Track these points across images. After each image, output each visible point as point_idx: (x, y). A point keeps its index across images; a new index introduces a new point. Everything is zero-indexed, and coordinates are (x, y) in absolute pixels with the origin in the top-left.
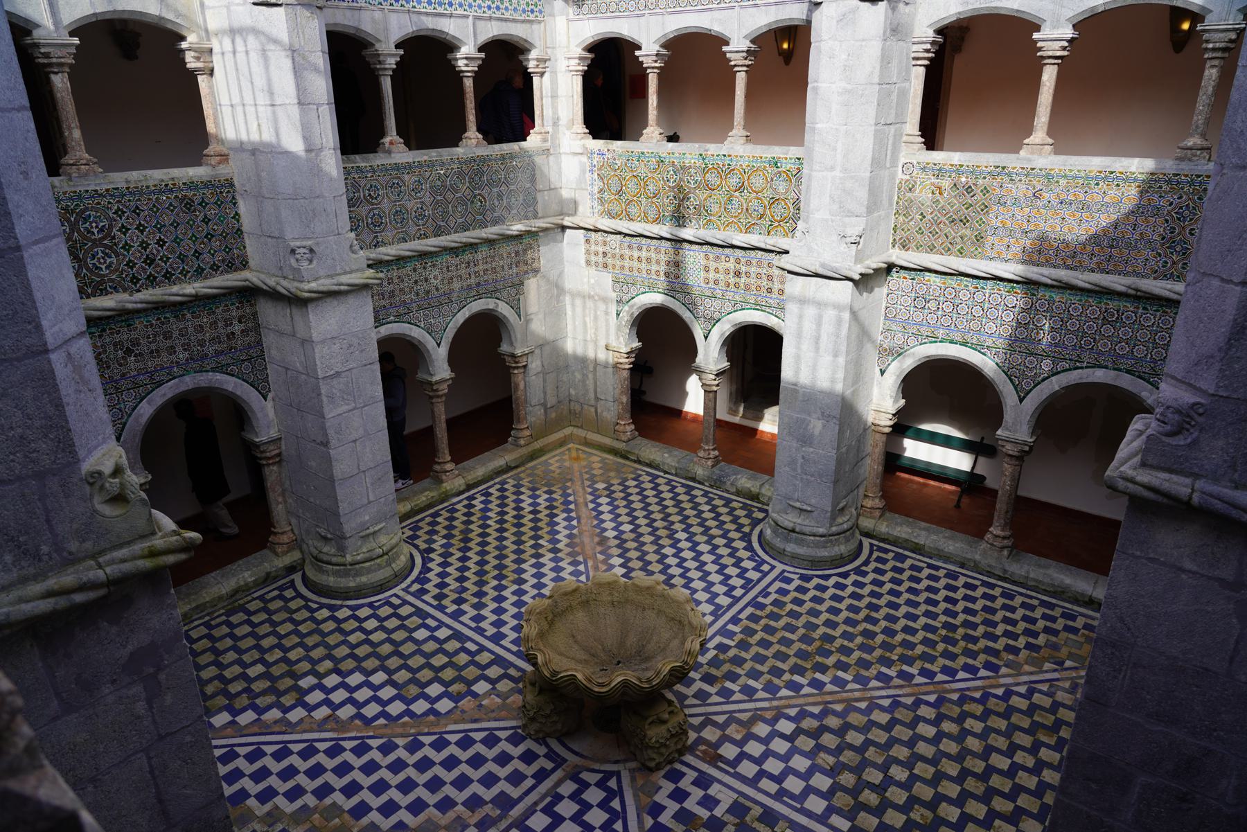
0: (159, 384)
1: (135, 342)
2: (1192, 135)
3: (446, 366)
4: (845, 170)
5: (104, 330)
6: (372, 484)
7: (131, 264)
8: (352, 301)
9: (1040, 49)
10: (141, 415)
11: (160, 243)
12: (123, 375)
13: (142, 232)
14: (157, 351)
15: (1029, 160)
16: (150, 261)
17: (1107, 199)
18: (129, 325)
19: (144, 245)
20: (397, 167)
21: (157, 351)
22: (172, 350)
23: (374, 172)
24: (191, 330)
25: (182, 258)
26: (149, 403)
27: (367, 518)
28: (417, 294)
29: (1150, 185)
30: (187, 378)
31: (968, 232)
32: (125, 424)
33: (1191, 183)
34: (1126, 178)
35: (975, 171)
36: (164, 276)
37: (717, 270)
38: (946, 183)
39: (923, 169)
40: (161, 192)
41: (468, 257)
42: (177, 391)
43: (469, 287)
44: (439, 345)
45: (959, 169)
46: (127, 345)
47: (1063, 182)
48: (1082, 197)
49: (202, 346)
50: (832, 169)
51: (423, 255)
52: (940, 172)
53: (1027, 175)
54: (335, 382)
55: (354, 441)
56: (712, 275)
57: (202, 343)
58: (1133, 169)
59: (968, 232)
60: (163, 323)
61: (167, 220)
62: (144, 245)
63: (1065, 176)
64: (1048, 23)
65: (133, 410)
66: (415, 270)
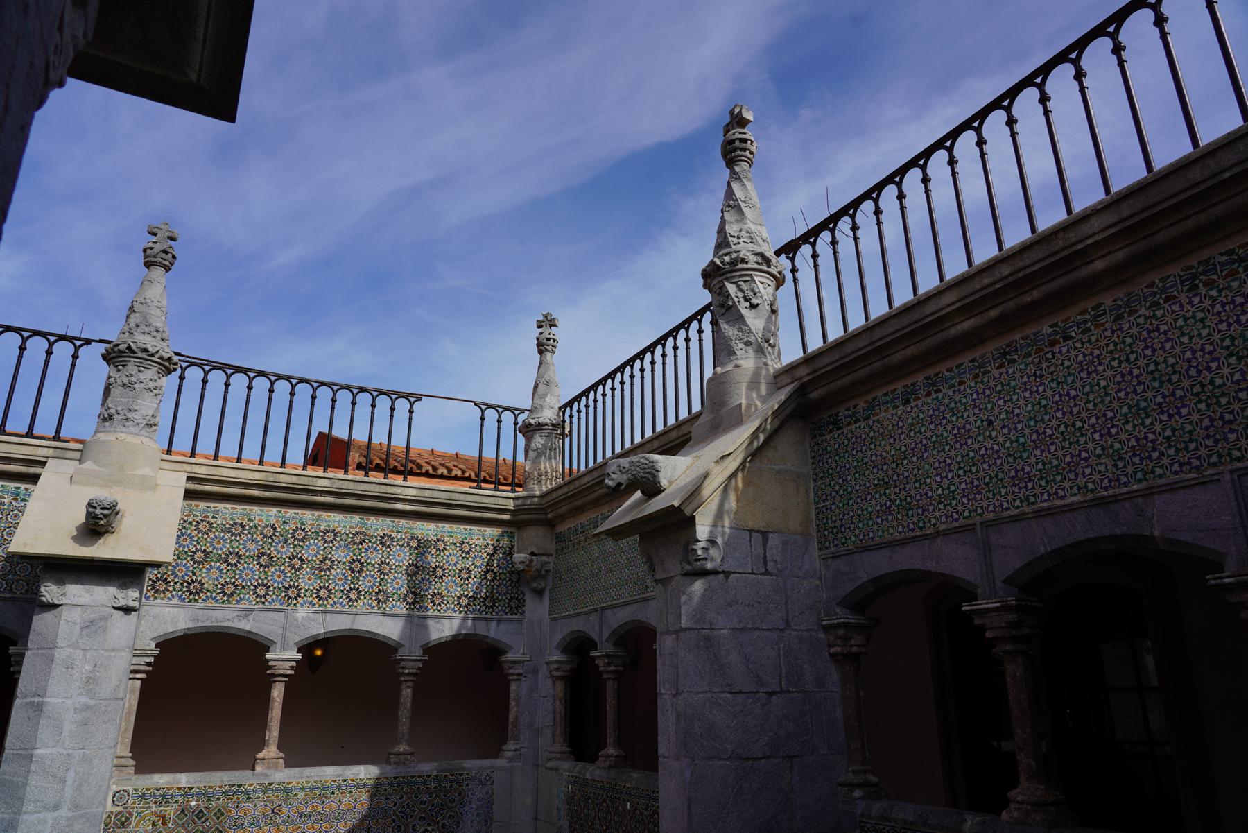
2: (400, 743)
4: (76, 807)
9: (271, 668)
15: (266, 775)
17: (343, 807)
29: (378, 790)
33: (408, 784)
34: (358, 785)
35: (207, 793)
38: (171, 811)
39: (142, 796)
45: (187, 793)
47: (301, 794)
48: (320, 808)
50: (56, 807)
52: (164, 797)
53: (265, 791)
58: (362, 776)
63: (303, 789)
64: (278, 645)
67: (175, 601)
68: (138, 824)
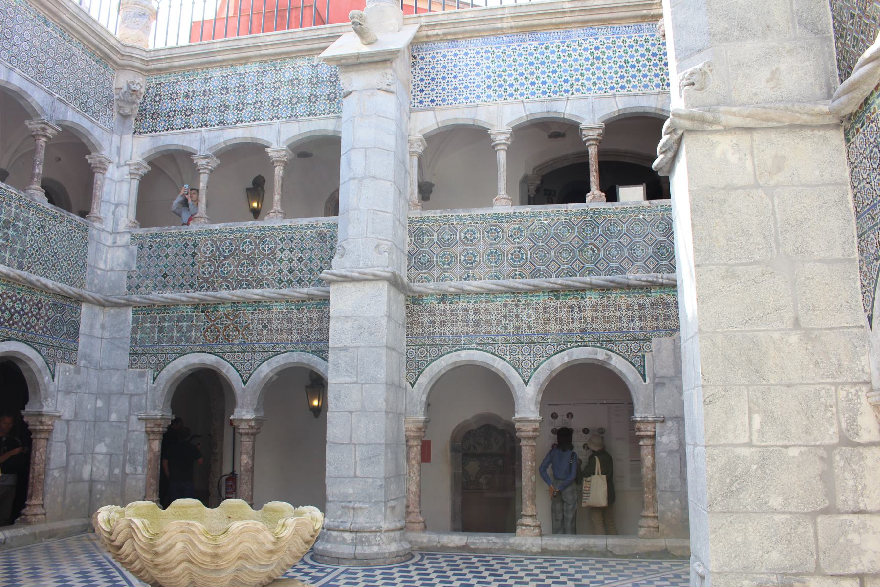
0: (277, 353)
1: (270, 321)
6: (361, 460)
7: (280, 271)
8: (368, 287)
10: (261, 372)
11: (300, 260)
12: (258, 341)
13: (292, 252)
14: (281, 330)
16: (291, 271)
19: (291, 260)
20: (497, 217)
21: (281, 330)
23: (473, 219)
24: (304, 320)
25: (311, 271)
26: (268, 364)
27: (351, 491)
28: (505, 328)
30: (295, 354)
32: (251, 375)
36: (298, 281)
40: (308, 228)
41: (571, 301)
42: (287, 362)
43: (571, 332)
44: (526, 383)
46: (265, 322)
49: (309, 333)
51: (515, 292)
54: (342, 354)
55: (351, 412)
57: (310, 331)
60: (289, 312)
61: (307, 246)
66: (505, 306)
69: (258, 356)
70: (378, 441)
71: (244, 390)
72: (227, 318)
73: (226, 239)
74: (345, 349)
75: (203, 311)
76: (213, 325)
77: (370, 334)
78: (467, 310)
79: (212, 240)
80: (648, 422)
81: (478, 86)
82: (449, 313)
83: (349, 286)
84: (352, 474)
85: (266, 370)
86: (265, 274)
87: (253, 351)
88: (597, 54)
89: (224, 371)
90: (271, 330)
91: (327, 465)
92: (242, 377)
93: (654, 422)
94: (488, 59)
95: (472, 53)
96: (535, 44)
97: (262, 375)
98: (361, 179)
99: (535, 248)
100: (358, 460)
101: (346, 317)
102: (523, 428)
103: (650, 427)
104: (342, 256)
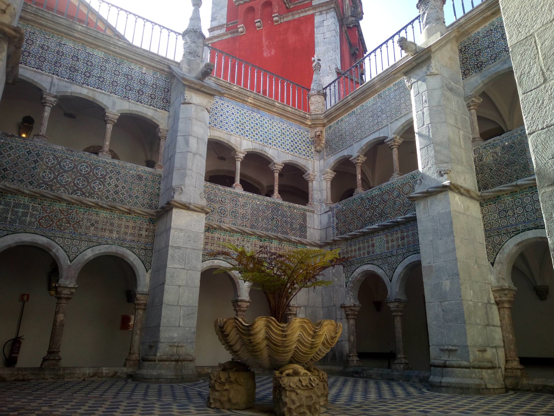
0: (100, 244)
3: (247, 295)
5: (86, 212)
6: (184, 316)
7: (108, 191)
10: (86, 255)
12: (86, 234)
14: (105, 230)
18: (97, 214)
19: (116, 186)
22: (111, 231)
23: (226, 192)
26: (92, 251)
27: (176, 335)
30: (113, 247)
31: (518, 167)
32: (77, 256)
37: (392, 241)
42: (107, 251)
54: (177, 250)
55: (180, 286)
56: (390, 244)
59: (518, 167)
62: (116, 186)
65: (84, 251)
67: (474, 74)
68: (486, 158)
69: (84, 244)
70: (194, 305)
71: (70, 267)
72: (61, 213)
73: (67, 158)
74: (179, 248)
75: (39, 204)
76: (48, 216)
77: (194, 242)
78: (220, 239)
79: (54, 156)
80: (295, 307)
81: (233, 125)
82: (210, 238)
83: (184, 212)
84: (177, 325)
85: (89, 254)
86: (96, 190)
87: (81, 240)
88: (283, 131)
89: (54, 251)
90: (97, 228)
91: (162, 318)
92: (69, 257)
93: (297, 307)
94: (238, 113)
95: (231, 107)
96: (259, 115)
97: (86, 258)
98: (195, 154)
99: (252, 214)
100: (181, 316)
101: (181, 229)
102: (242, 306)
103: (295, 309)
104: (180, 194)
